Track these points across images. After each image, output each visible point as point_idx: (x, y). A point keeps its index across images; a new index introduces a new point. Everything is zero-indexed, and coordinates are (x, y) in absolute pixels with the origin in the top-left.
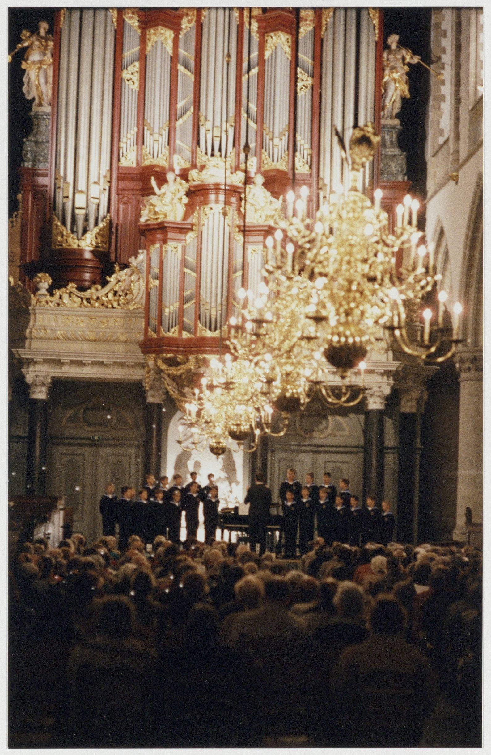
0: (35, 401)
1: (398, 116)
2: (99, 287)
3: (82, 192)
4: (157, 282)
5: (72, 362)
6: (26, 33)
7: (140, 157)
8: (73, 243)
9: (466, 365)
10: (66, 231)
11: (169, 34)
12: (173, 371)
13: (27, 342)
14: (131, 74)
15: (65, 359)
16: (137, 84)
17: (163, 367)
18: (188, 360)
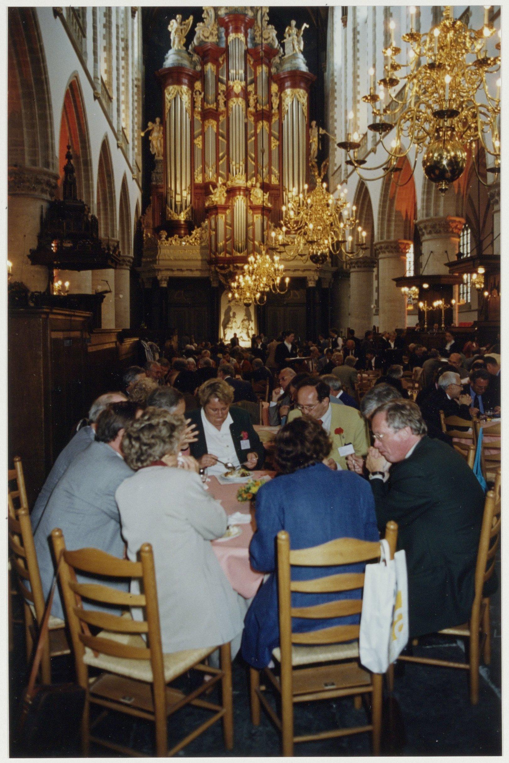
0: (162, 288)
1: (316, 158)
2: (188, 236)
4: (214, 233)
5: (178, 270)
6: (150, 124)
7: (204, 179)
8: (176, 217)
9: (353, 265)
10: (173, 212)
11: (214, 123)
12: (223, 272)
13: (157, 262)
14: (198, 141)
15: (175, 269)
16: (201, 146)
17: (218, 270)
18: (229, 267)
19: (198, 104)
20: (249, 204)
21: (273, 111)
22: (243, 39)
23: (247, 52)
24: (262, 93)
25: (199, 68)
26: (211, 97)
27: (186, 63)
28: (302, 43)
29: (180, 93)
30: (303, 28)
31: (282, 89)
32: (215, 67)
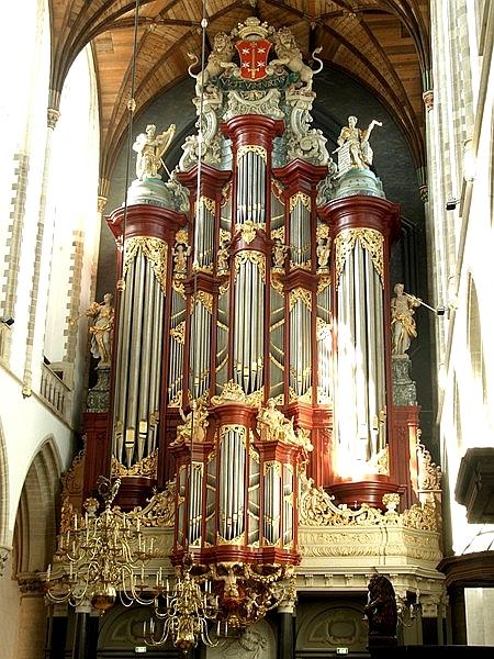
0: (81, 614)
3: (132, 428)
11: (209, 297)
14: (178, 333)
16: (183, 340)
19: (180, 268)
20: (252, 441)
21: (320, 271)
22: (263, 154)
23: (269, 172)
24: (296, 239)
25: (185, 207)
26: (199, 255)
27: (161, 199)
28: (370, 149)
29: (145, 249)
30: (371, 127)
31: (334, 234)
32: (214, 202)
